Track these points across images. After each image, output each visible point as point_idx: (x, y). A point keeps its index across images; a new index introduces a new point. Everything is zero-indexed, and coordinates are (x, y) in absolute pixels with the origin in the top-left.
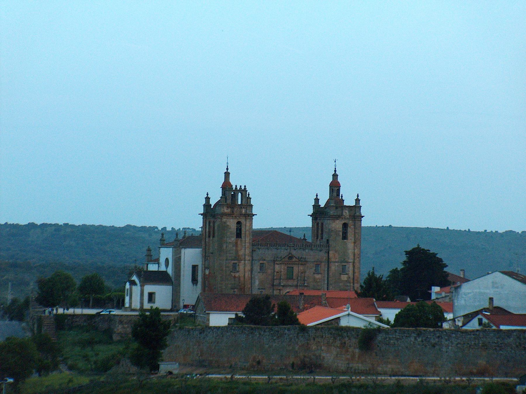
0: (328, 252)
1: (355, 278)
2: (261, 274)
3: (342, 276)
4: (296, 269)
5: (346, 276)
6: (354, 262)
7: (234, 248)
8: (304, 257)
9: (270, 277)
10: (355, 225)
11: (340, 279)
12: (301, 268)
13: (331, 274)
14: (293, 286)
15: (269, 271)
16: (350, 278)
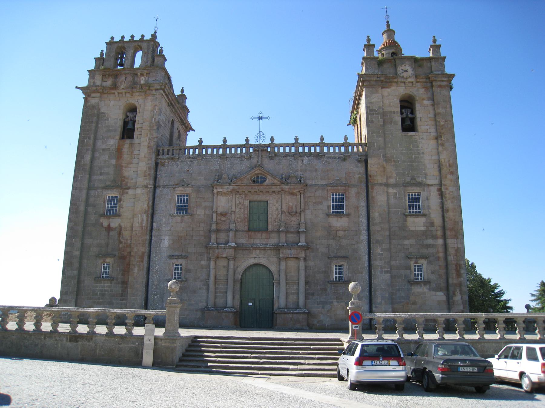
0: (366, 162)
1: (449, 225)
2: (179, 219)
3: (410, 219)
4: (276, 206)
5: (423, 220)
6: (441, 185)
7: (113, 162)
8: (299, 173)
9: (203, 228)
10: (432, 99)
11: (403, 227)
13: (375, 215)
14: (264, 249)
15: (200, 213)
16: (432, 224)
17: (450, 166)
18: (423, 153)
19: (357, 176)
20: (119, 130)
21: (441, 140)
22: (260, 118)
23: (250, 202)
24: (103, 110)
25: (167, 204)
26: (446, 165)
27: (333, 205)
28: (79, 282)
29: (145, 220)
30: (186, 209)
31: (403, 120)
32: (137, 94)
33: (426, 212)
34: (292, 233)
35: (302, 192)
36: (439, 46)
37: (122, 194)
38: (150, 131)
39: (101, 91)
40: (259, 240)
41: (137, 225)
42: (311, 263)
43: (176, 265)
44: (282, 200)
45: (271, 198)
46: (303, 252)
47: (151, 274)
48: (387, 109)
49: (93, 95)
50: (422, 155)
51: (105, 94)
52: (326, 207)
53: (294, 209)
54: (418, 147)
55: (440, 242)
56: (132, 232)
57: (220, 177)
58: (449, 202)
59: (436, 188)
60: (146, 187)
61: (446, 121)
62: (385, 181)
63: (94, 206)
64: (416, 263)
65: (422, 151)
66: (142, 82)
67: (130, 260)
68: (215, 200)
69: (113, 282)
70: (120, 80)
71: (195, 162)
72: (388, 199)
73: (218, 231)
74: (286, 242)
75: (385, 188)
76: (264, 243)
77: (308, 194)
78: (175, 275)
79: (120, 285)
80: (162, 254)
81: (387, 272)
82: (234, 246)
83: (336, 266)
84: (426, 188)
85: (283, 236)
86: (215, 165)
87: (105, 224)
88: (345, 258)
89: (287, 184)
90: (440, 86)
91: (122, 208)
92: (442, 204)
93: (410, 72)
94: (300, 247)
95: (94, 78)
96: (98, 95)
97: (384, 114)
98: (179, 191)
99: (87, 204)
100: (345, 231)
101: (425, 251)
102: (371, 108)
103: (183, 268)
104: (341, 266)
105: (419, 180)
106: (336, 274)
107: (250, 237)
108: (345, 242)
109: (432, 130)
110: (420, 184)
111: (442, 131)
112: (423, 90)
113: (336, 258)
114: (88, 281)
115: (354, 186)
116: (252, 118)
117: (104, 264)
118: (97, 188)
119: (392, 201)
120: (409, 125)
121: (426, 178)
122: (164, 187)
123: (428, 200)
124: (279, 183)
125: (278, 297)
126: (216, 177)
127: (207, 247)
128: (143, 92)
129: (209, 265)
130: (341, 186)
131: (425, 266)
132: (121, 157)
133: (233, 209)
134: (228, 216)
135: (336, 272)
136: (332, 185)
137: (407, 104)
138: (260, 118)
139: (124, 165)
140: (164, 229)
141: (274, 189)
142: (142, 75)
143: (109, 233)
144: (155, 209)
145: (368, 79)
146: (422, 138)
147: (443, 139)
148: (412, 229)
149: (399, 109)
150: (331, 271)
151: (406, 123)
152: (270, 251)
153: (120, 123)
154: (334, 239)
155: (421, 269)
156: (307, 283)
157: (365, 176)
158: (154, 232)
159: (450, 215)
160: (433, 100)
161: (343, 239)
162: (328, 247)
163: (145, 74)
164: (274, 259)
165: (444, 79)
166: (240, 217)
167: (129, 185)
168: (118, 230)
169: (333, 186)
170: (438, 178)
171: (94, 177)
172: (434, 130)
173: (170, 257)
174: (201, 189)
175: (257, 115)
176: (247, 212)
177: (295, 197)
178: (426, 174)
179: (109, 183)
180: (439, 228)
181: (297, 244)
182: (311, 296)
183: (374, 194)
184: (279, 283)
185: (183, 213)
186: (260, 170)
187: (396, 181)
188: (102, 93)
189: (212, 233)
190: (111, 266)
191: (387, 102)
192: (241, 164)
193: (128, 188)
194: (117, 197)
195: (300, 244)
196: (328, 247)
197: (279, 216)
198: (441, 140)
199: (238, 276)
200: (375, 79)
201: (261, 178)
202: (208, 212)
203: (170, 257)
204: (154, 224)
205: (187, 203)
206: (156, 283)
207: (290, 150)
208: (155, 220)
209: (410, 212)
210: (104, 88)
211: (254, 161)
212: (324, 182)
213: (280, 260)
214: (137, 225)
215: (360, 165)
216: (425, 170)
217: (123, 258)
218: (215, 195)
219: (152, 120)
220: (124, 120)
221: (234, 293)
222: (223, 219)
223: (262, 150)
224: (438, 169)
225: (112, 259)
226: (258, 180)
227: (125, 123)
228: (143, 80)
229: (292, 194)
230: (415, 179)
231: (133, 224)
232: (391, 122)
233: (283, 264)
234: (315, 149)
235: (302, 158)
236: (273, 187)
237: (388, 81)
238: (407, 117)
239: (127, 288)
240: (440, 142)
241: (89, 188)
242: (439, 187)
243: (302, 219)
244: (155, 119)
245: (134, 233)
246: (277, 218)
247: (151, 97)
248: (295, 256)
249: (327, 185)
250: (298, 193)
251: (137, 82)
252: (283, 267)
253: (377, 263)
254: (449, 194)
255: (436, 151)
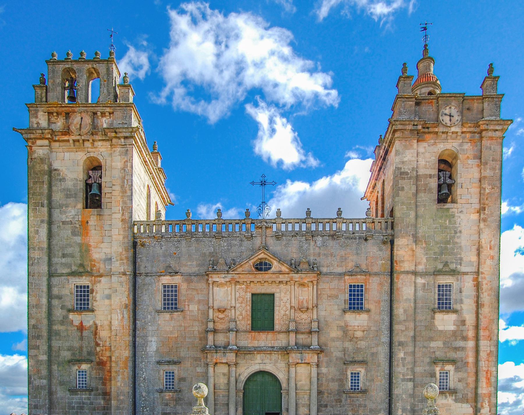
0: (392, 243)
1: (483, 323)
2: (167, 316)
3: (439, 316)
5: (453, 317)
8: (312, 258)
9: (197, 328)
11: (430, 326)
12: (306, 295)
13: (400, 311)
15: (193, 308)
16: (463, 323)
17: (490, 248)
18: (460, 232)
19: (380, 262)
20: (81, 195)
21: (484, 214)
22: (263, 184)
23: (253, 295)
24: (56, 165)
25: (153, 298)
26: (487, 247)
27: (350, 299)
28: (51, 393)
29: (126, 316)
30: (176, 304)
31: (440, 186)
32: (100, 143)
33: (457, 307)
34: (303, 333)
35: (315, 282)
36: (497, 78)
37: (95, 283)
38: (122, 197)
39: (49, 136)
40: (264, 340)
41: (116, 323)
42: (324, 370)
43: (166, 373)
44: (290, 292)
45: (278, 290)
46: (316, 357)
47: (137, 384)
48: (421, 172)
49: (39, 142)
50: (458, 234)
51: (55, 141)
52: (343, 301)
53: (305, 305)
54: (455, 223)
55: (471, 344)
56: (111, 332)
57: (215, 263)
58: (485, 294)
59: (472, 277)
60: (124, 274)
61: (493, 188)
62: (413, 268)
63: (59, 297)
64: (442, 369)
65: (459, 229)
66: (105, 126)
67: (111, 367)
68: (211, 292)
69: (93, 393)
70: (75, 122)
71: (184, 243)
72: (415, 290)
73: (215, 331)
74: (296, 345)
75: (413, 277)
76: (270, 345)
77: (322, 286)
78: (166, 385)
79: (100, 397)
80: (150, 359)
81: (410, 380)
82: (236, 350)
83: (352, 373)
84: (459, 277)
85: (292, 336)
86: (208, 247)
87: (77, 323)
88: (363, 362)
89: (297, 273)
90: (491, 138)
91: (96, 301)
92: (478, 297)
93: (457, 117)
94: (313, 350)
95: (37, 117)
96: (46, 142)
97: (418, 178)
98: (166, 280)
99: (50, 296)
100: (364, 331)
101: (452, 355)
102: (403, 170)
103: (176, 377)
104: (358, 373)
105: (453, 266)
106: (352, 383)
107: (254, 338)
108: (362, 344)
109: (475, 200)
110: (454, 273)
111: (487, 202)
112: (469, 144)
113: (354, 362)
114: (60, 393)
115: (376, 274)
116: (253, 183)
117: (79, 372)
118: (62, 275)
119: (420, 293)
120: (445, 194)
121: (461, 265)
122: (147, 275)
123: (461, 292)
124: (287, 270)
125: (287, 410)
126: (211, 262)
127: (204, 350)
128: (108, 140)
129: (207, 373)
130: (361, 275)
131: (452, 373)
132: (87, 233)
133: (234, 305)
134: (225, 313)
135: (352, 380)
136: (351, 273)
137: (446, 165)
138: (263, 184)
139: (92, 244)
140: (150, 328)
141: (282, 278)
142: (103, 114)
143: (82, 333)
144: (137, 303)
145: (400, 127)
146: (461, 212)
147: (486, 212)
148: (440, 328)
149: (435, 172)
150: (347, 378)
151: (443, 192)
152: (277, 355)
153: (81, 186)
154: (351, 341)
155: (447, 376)
156: (320, 393)
157: (389, 262)
158: (138, 332)
159: (485, 311)
160: (480, 159)
161: (361, 340)
162: (344, 350)
163: (107, 114)
164: (282, 365)
165: (497, 128)
166: (241, 314)
167: (101, 271)
168: (93, 329)
169: (351, 275)
170: (475, 264)
171: (55, 260)
172: (477, 201)
173: (159, 363)
174: (193, 277)
175: (258, 179)
176: (249, 308)
177: (306, 289)
178: (461, 259)
179: (76, 268)
180: (471, 328)
181: (309, 347)
182: (323, 409)
183: (400, 285)
184: (288, 394)
185: (172, 308)
186: (265, 254)
187: (426, 269)
188: (51, 140)
189: (209, 333)
190: (88, 373)
191: (422, 162)
192: (241, 245)
193: (101, 276)
194: (88, 287)
195: (312, 347)
196: (344, 350)
197: (287, 312)
198: (484, 214)
199: (241, 386)
200: (410, 127)
201: (266, 264)
202: (201, 307)
203: (159, 363)
204: (137, 322)
205: (176, 296)
206: (144, 394)
207: (300, 227)
208: (137, 318)
209: (439, 308)
210: (53, 132)
211: (258, 242)
212: (340, 270)
213: (289, 365)
214: (117, 322)
215: (384, 247)
216: (460, 254)
217: (101, 364)
218: (211, 286)
219: (124, 182)
220: (86, 181)
221: (236, 405)
222: (221, 316)
223: (266, 228)
224: (476, 253)
225: (89, 365)
226: (262, 267)
227: (88, 186)
228: (104, 122)
229: (302, 285)
230: (448, 266)
231: (111, 322)
232: (425, 190)
233: (293, 370)
234: (331, 227)
235: (314, 239)
236: (281, 276)
237: (426, 130)
238: (444, 183)
239: (110, 400)
240: (482, 216)
241: (51, 275)
242: (475, 276)
243: (315, 317)
244: (127, 180)
245: (113, 333)
246: (285, 315)
247: (119, 149)
248: (306, 361)
249: (344, 274)
250: (310, 284)
251: (97, 126)
252: (293, 375)
253: (400, 370)
254: (487, 284)
255: (476, 228)
